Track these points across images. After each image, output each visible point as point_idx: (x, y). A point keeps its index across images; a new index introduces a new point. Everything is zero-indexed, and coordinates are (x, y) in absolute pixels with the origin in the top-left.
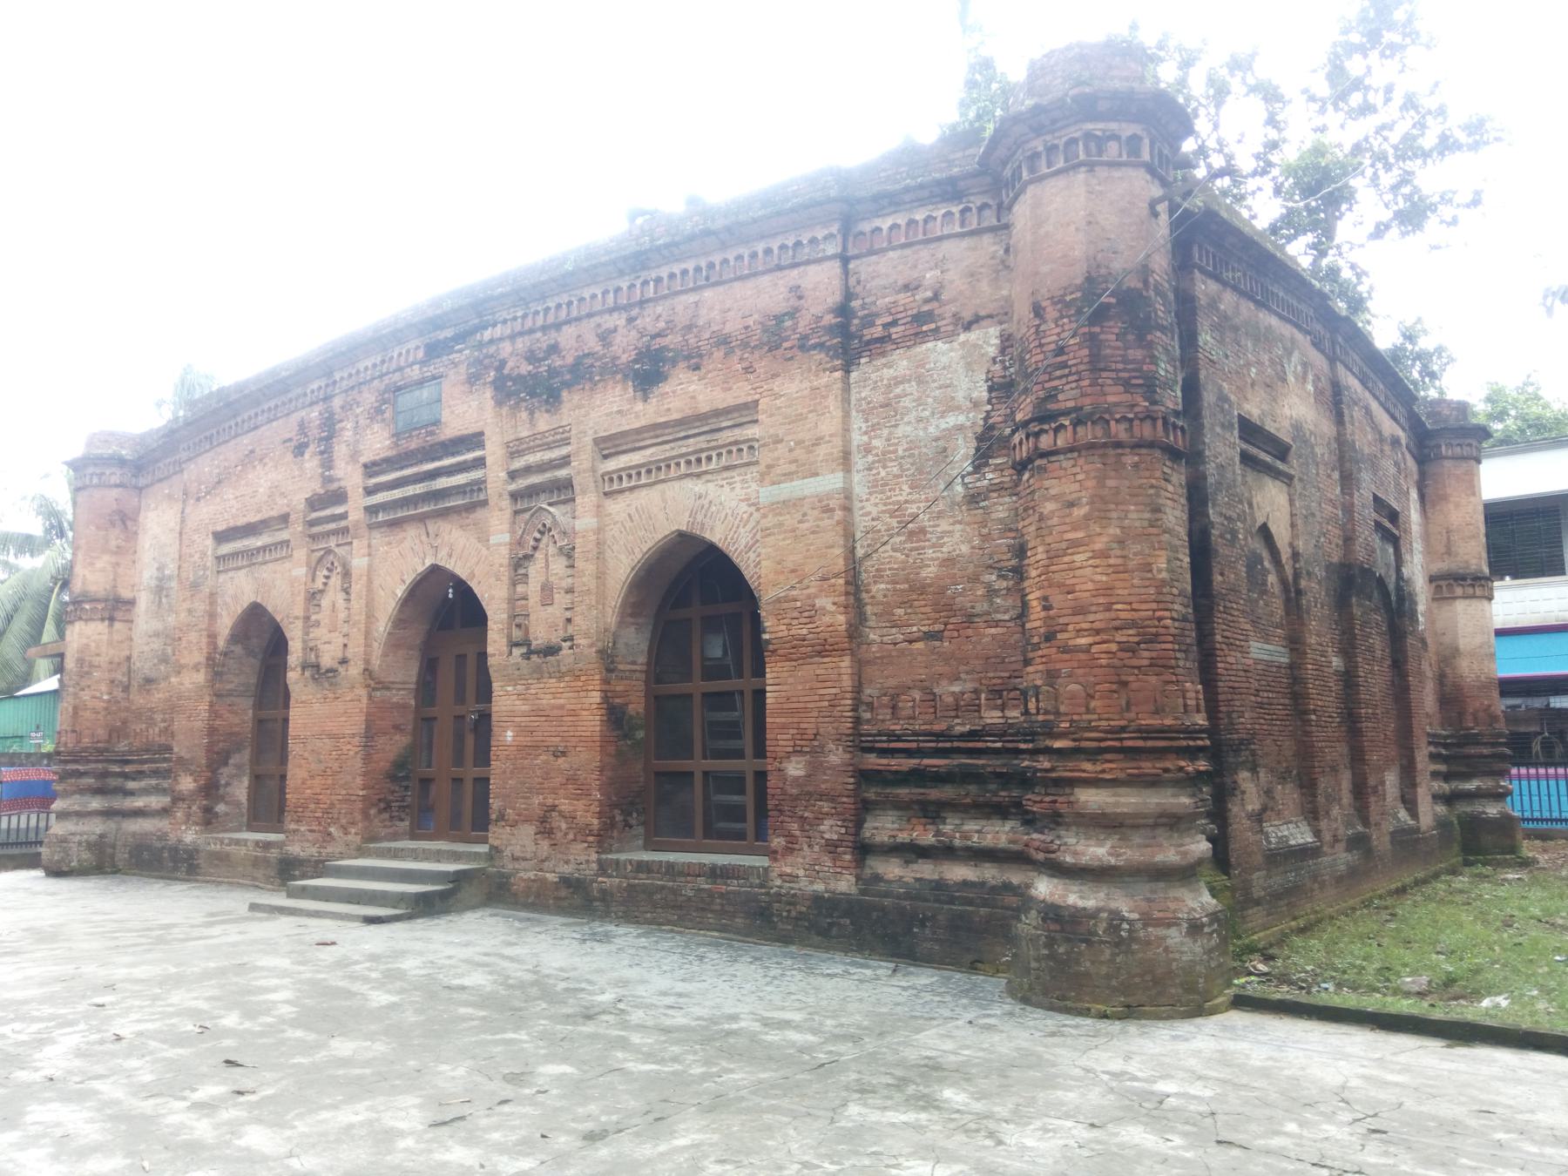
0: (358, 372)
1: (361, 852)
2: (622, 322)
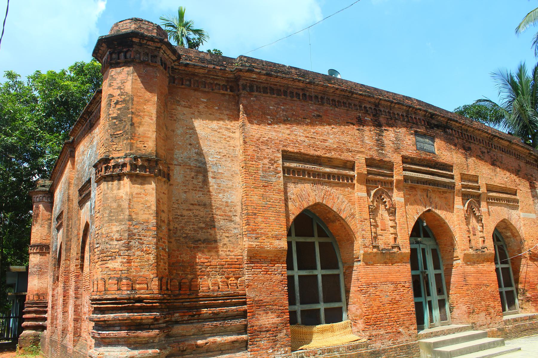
0: (394, 114)
1: (418, 337)
2: (486, 151)
